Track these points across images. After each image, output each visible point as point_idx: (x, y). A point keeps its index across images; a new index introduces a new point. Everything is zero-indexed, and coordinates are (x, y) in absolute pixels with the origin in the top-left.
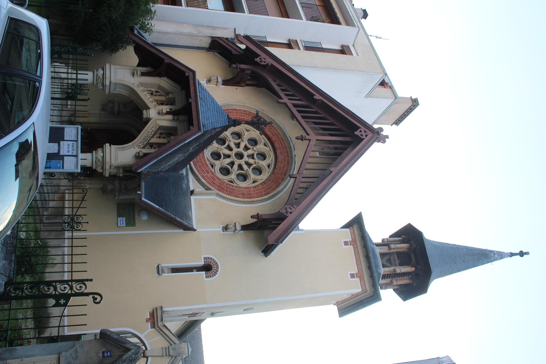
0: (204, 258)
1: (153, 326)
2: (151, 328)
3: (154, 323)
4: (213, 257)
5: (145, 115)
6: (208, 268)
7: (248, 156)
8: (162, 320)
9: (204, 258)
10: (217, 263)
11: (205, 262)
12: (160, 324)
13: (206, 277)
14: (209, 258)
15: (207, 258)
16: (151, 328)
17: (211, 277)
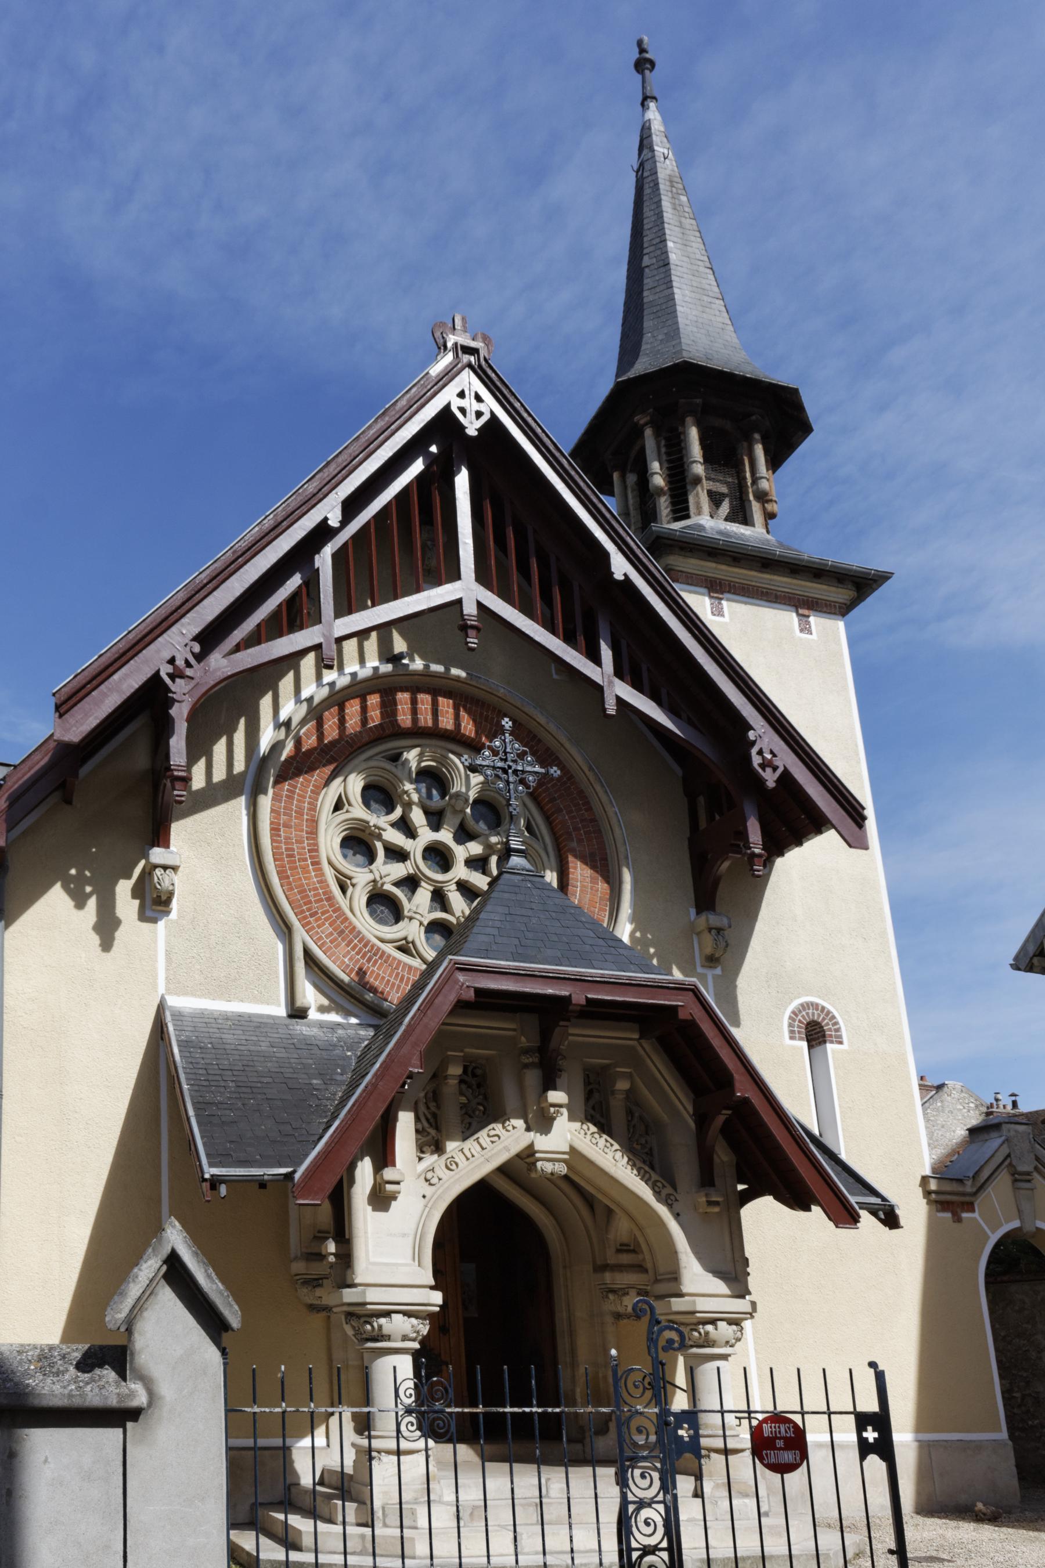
0: (791, 1038)
1: (970, 1207)
2: (973, 1211)
3: (963, 1203)
4: (788, 1013)
5: (562, 1169)
6: (815, 1033)
7: (436, 827)
8: (960, 1181)
9: (791, 1038)
10: (802, 1005)
11: (801, 1039)
12: (969, 1188)
13: (841, 1043)
14: (790, 1025)
15: (792, 1032)
16: (973, 1211)
17: (838, 1030)
